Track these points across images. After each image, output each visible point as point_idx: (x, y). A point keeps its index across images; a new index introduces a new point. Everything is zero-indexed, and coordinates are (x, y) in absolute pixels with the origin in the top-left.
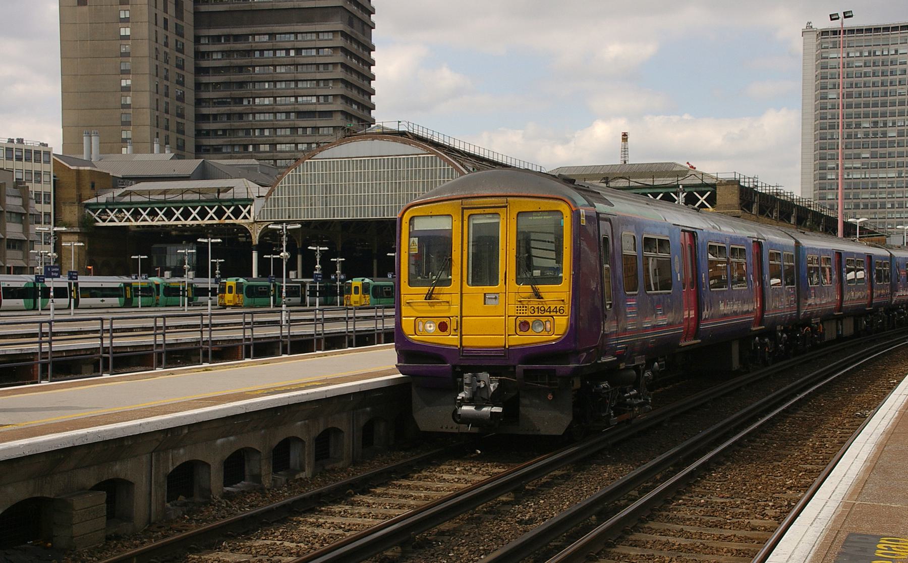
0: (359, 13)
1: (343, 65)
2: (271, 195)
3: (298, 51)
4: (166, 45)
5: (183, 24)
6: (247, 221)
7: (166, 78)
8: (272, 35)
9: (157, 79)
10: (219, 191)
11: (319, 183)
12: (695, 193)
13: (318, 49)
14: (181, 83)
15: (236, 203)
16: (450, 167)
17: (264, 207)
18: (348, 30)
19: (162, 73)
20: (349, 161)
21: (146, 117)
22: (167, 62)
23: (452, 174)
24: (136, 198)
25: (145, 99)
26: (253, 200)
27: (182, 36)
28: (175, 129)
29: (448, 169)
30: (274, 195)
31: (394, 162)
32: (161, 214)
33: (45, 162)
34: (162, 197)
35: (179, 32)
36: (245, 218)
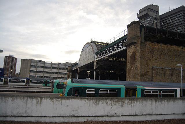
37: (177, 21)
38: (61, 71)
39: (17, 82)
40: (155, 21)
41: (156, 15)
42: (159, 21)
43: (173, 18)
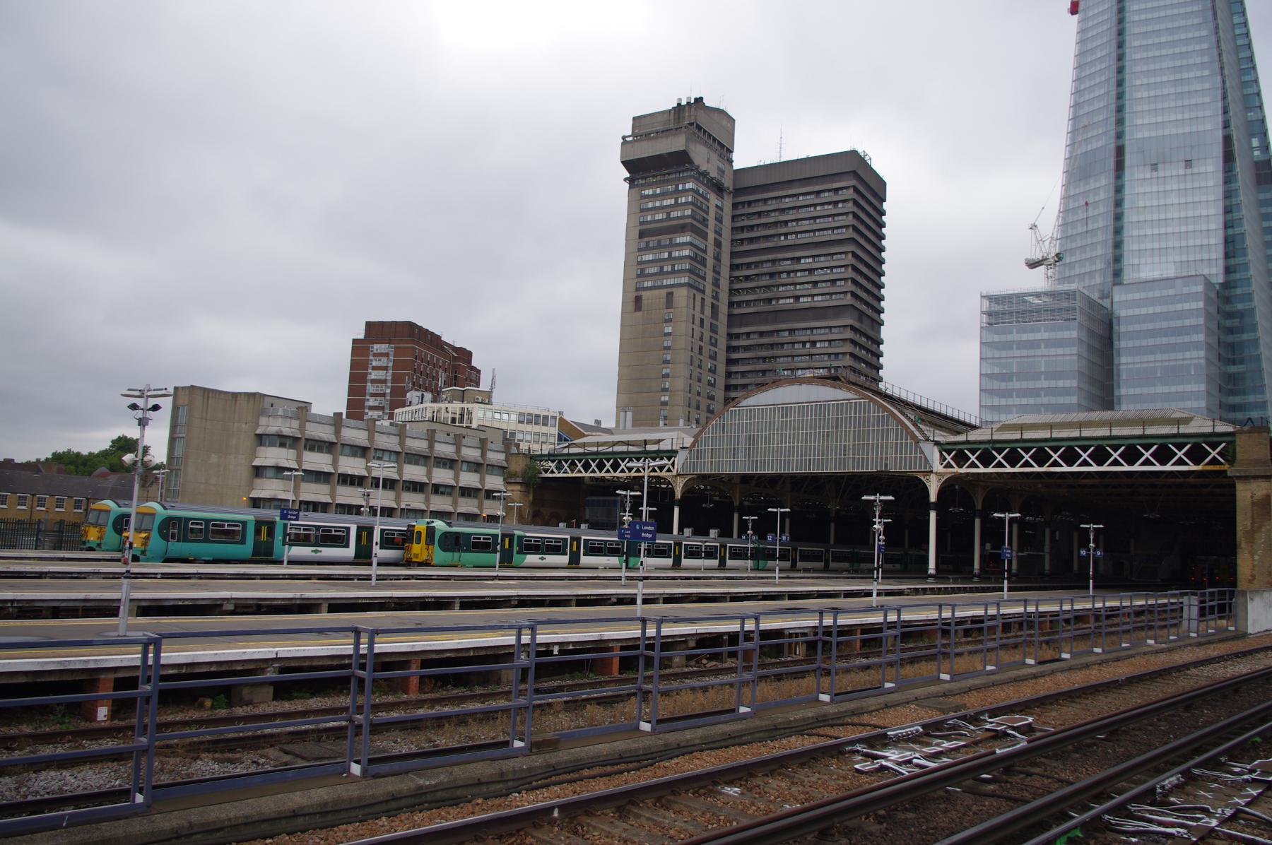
0: (869, 312)
1: (852, 355)
2: (694, 446)
3: (813, 343)
4: (701, 339)
5: (718, 324)
6: (670, 474)
7: (700, 367)
8: (791, 331)
9: (691, 368)
10: (646, 442)
11: (742, 432)
12: (1203, 445)
13: (830, 341)
14: (713, 371)
17: (687, 459)
18: (857, 325)
19: (697, 362)
21: (681, 398)
22: (701, 353)
24: (573, 450)
25: (680, 384)
26: (676, 452)
27: (716, 333)
28: (705, 409)
29: (883, 416)
31: (822, 408)
32: (579, 465)
33: (551, 426)
34: (594, 449)
35: (714, 329)
36: (669, 470)
37: (820, 224)
38: (442, 476)
39: (206, 541)
40: (714, 200)
41: (719, 169)
42: (727, 203)
43: (803, 200)
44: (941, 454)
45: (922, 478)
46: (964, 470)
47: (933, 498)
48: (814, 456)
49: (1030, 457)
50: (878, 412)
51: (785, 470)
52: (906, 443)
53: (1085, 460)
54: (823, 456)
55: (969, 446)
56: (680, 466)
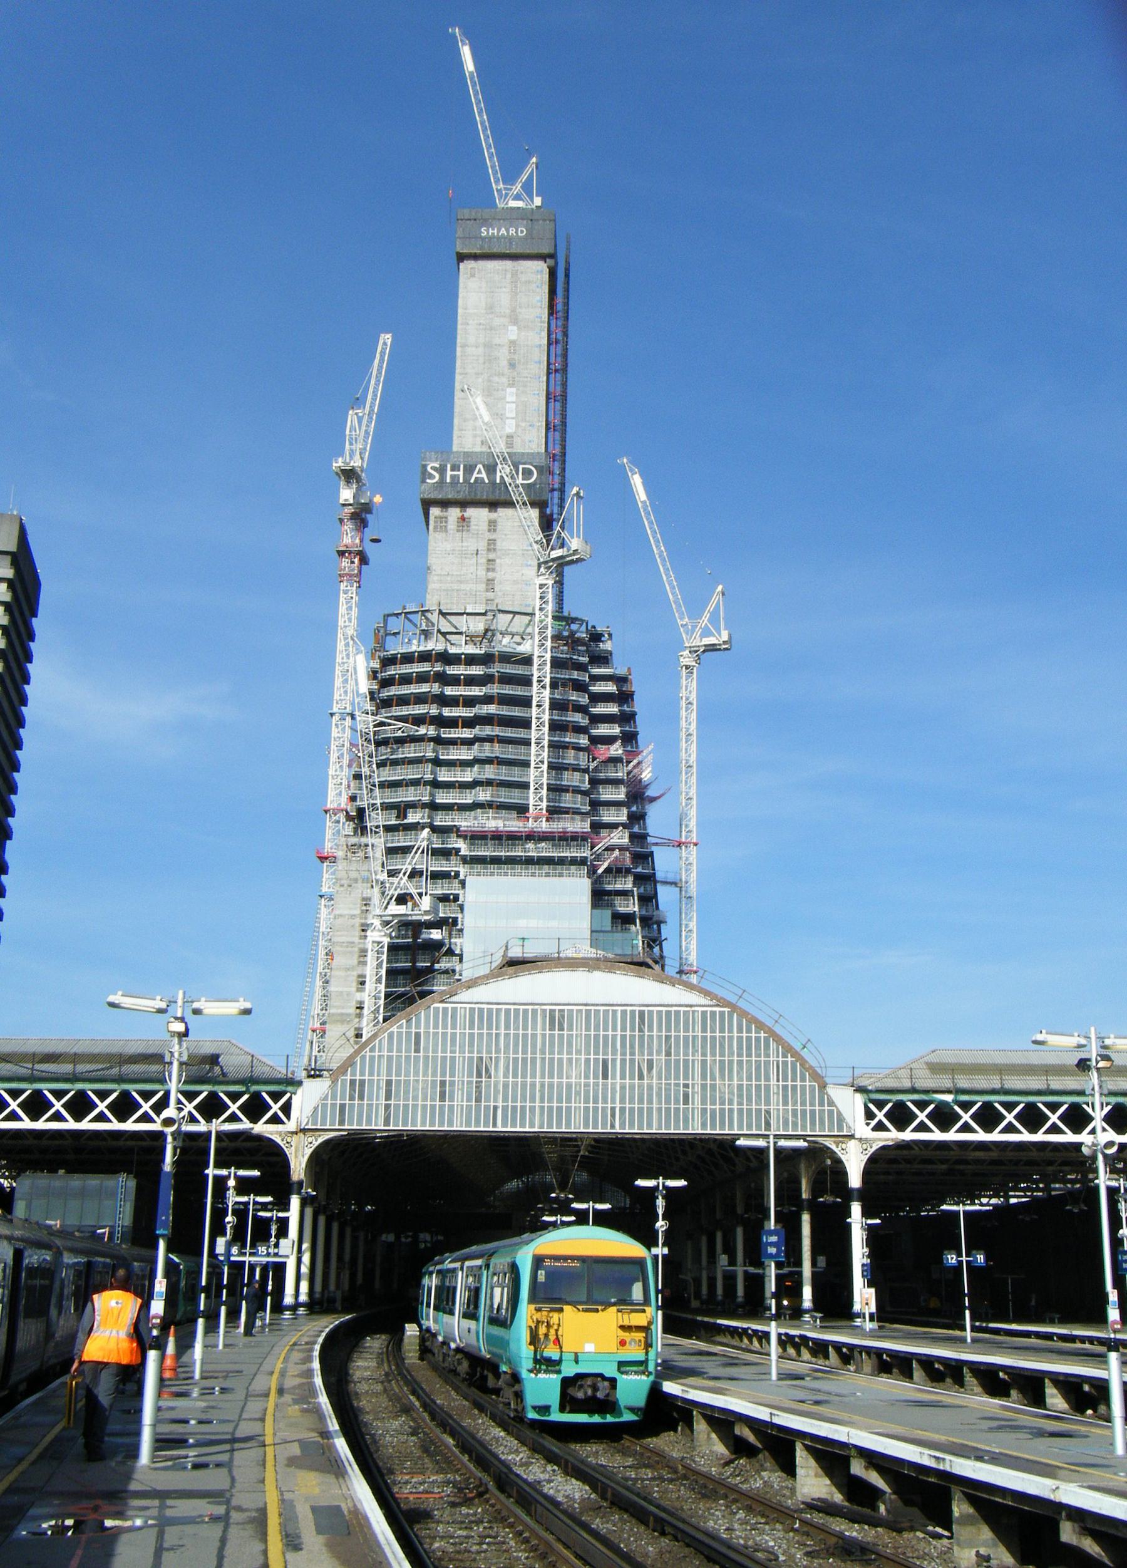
2: (344, 1073)
6: (280, 1127)
15: (254, 1088)
16: (762, 1035)
17: (326, 1098)
20: (534, 1012)
23: (767, 1046)
29: (758, 1039)
30: (353, 1074)
36: (275, 1120)
44: (867, 1108)
45: (833, 1147)
46: (908, 1135)
47: (855, 1180)
48: (622, 1101)
49: (973, 1117)
50: (749, 1031)
51: (559, 1125)
52: (803, 1088)
53: (1054, 1124)
54: (641, 1101)
55: (916, 1097)
56: (308, 1111)
